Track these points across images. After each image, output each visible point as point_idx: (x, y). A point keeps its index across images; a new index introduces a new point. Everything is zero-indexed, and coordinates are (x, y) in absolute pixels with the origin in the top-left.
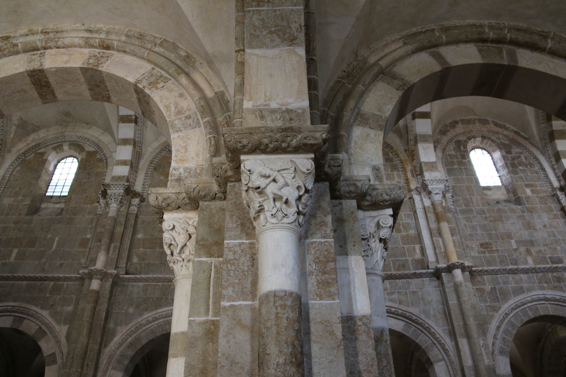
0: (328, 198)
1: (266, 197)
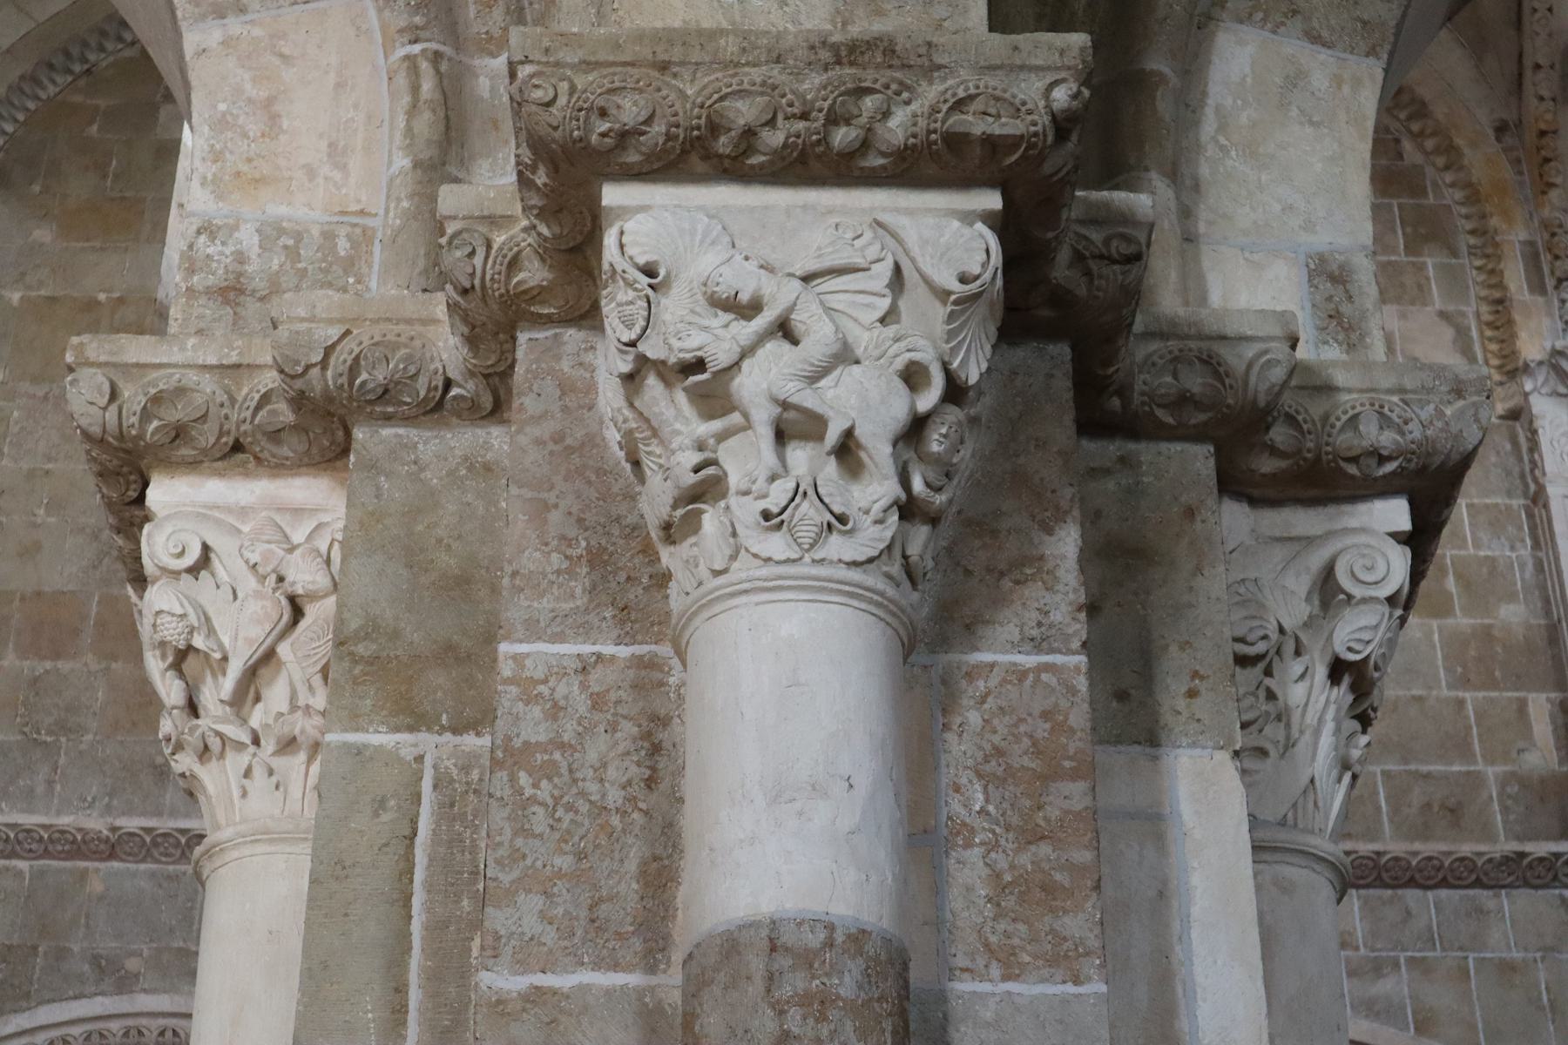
0: (1062, 430)
1: (736, 418)
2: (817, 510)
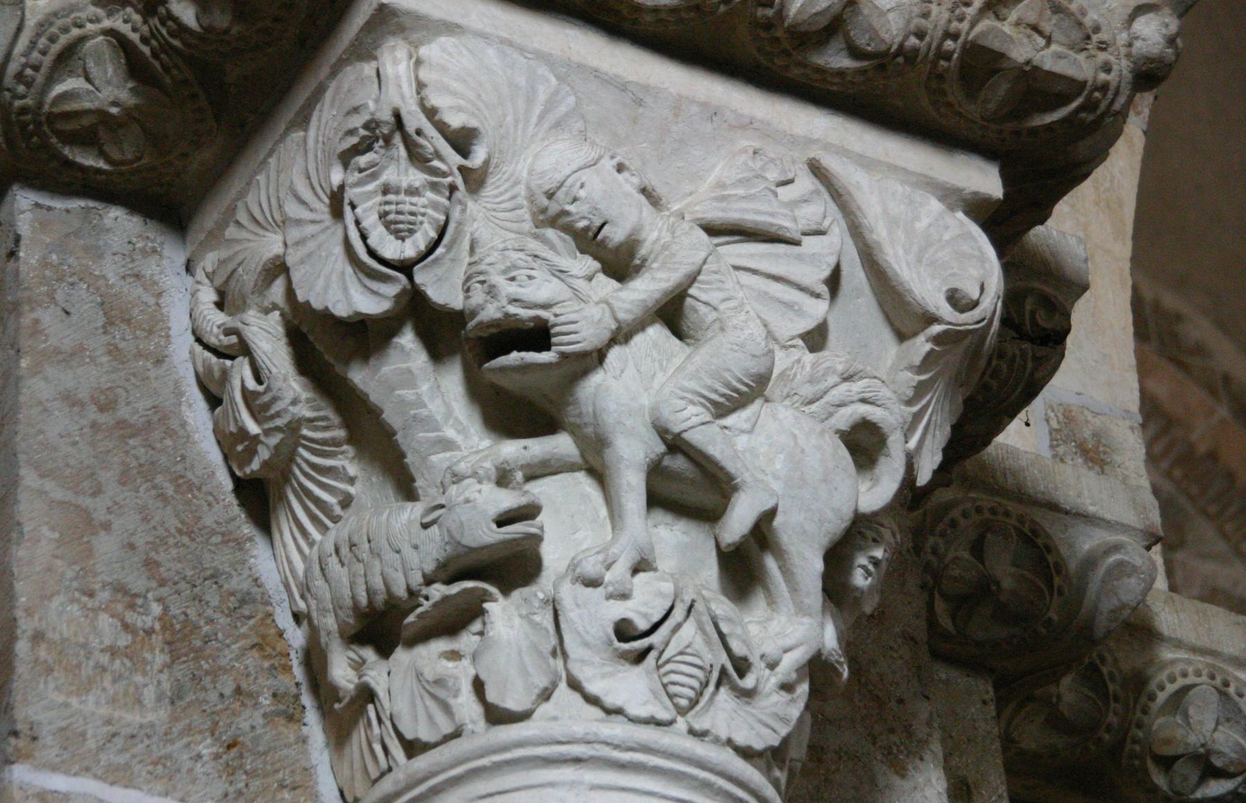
2: (708, 642)
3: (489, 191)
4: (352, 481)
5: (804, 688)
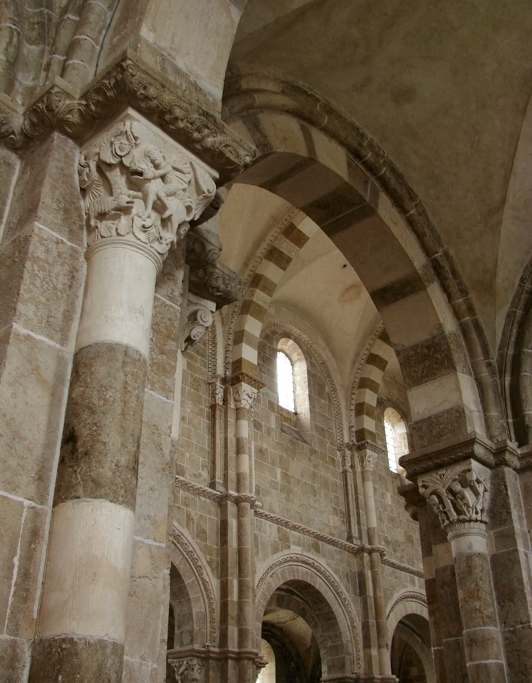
3: (138, 149)
4: (101, 192)
5: (169, 246)
